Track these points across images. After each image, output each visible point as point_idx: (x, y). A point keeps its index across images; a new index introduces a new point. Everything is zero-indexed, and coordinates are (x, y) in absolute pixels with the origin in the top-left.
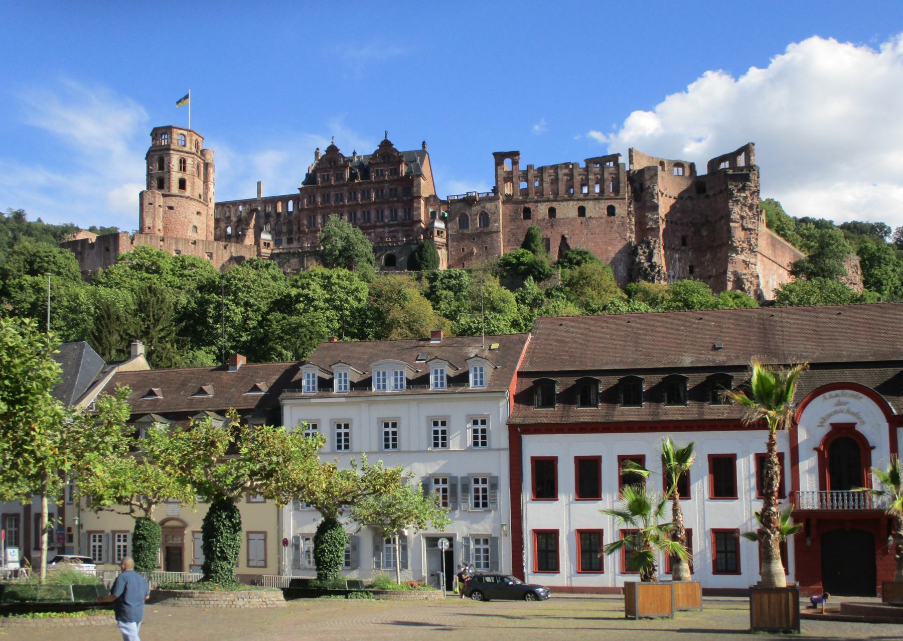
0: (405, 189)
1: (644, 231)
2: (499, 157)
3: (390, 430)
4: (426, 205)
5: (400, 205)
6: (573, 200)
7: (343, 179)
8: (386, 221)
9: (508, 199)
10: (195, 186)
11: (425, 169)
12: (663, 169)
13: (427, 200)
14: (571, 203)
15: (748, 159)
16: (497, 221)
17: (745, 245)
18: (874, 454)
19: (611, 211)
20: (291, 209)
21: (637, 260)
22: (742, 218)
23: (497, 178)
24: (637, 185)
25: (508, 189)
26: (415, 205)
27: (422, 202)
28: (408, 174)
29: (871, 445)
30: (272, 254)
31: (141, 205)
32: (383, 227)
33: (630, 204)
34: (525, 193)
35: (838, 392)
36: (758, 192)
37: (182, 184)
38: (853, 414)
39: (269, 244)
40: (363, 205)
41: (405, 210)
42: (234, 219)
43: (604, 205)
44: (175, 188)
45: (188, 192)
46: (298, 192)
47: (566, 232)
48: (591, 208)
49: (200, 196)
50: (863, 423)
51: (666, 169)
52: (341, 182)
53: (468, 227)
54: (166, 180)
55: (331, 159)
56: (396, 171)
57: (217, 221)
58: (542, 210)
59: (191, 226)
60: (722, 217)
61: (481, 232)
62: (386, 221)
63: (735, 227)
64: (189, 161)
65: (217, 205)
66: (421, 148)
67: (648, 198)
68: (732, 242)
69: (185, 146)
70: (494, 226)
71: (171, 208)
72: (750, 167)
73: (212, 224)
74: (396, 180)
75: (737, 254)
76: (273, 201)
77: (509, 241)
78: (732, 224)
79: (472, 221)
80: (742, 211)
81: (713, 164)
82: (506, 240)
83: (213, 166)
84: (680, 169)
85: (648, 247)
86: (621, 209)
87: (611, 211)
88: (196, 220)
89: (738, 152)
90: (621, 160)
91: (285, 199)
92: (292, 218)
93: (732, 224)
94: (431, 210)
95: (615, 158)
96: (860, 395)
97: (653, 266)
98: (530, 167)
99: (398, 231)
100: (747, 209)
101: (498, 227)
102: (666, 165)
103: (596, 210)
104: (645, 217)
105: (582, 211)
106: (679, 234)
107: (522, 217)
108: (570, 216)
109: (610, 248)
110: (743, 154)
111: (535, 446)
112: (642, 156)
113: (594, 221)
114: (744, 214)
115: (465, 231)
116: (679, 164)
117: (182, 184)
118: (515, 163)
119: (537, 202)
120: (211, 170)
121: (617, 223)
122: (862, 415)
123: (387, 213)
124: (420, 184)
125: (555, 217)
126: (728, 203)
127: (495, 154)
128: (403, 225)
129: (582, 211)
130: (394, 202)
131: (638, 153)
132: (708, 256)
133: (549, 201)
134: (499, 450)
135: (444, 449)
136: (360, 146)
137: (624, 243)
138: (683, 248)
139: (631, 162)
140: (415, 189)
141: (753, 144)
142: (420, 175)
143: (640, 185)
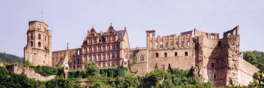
0: (117, 46)
1: (198, 61)
11: (125, 38)
13: (124, 50)
19: (186, 54)
22: (233, 56)
24: (196, 44)
28: (118, 40)
36: (239, 45)
37: (39, 44)
41: (117, 54)
43: (184, 52)
44: (37, 46)
48: (181, 53)
54: (33, 43)
60: (226, 56)
61: (141, 63)
63: (230, 60)
64: (42, 35)
66: (124, 29)
68: (229, 65)
79: (138, 58)
81: (225, 34)
82: (150, 66)
84: (214, 36)
85: (198, 68)
86: (190, 54)
87: (186, 54)
89: (234, 30)
93: (229, 58)
95: (190, 32)
97: (199, 76)
99: (114, 62)
100: (235, 53)
103: (181, 53)
105: (176, 54)
110: (235, 30)
113: (180, 58)
114: (233, 54)
116: (213, 34)
117: (39, 44)
125: (166, 56)
126: (228, 50)
128: (116, 60)
129: (176, 54)
130: (113, 51)
136: (102, 29)
140: (120, 46)
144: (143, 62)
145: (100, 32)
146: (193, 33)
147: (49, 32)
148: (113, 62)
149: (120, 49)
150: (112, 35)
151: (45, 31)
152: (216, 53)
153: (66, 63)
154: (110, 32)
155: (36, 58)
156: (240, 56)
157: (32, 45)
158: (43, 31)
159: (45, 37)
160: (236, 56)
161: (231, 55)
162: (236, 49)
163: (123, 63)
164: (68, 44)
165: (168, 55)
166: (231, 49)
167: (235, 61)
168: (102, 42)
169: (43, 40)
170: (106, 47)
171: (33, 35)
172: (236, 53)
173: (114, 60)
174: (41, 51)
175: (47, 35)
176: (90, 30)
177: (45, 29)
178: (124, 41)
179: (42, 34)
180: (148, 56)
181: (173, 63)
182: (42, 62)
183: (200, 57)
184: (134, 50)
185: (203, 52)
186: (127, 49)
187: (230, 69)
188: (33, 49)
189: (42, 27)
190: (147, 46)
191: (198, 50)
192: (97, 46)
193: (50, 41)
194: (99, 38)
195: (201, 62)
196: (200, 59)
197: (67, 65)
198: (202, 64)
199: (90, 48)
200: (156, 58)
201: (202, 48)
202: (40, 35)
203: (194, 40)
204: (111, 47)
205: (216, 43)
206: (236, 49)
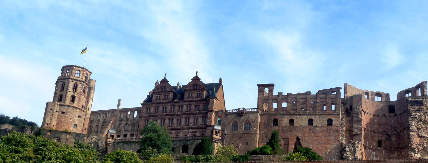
1: (352, 135)
2: (261, 87)
4: (216, 115)
5: (201, 115)
6: (306, 115)
10: (81, 101)
11: (218, 95)
12: (368, 98)
13: (216, 113)
14: (304, 116)
16: (256, 126)
17: (420, 147)
19: (330, 122)
20: (135, 116)
21: (345, 154)
22: (418, 129)
25: (265, 108)
26: (209, 115)
28: (206, 97)
31: (46, 110)
32: (188, 129)
33: (342, 118)
37: (73, 98)
39: (113, 136)
40: (177, 115)
41: (203, 118)
42: (101, 121)
43: (325, 118)
44: (68, 102)
45: (75, 104)
46: (141, 106)
47: (300, 135)
48: (319, 121)
49: (83, 107)
51: (370, 97)
53: (237, 130)
54: (64, 97)
56: (200, 95)
57: (91, 122)
58: (285, 121)
59: (73, 124)
60: (405, 129)
62: (191, 125)
63: (413, 135)
66: (218, 82)
69: (79, 77)
73: (87, 123)
74: (199, 101)
75: (415, 153)
76: (125, 111)
77: (263, 139)
78: (411, 133)
79: (240, 126)
80: (418, 125)
81: (402, 95)
82: (261, 139)
83: (94, 90)
84: (380, 98)
87: (330, 122)
88: (77, 121)
89: (418, 87)
91: (133, 110)
93: (411, 133)
94: (219, 119)
95: (337, 90)
98: (280, 94)
99: (196, 132)
101: (256, 131)
102: (370, 94)
104: (352, 127)
105: (311, 122)
106: (376, 139)
107: (272, 124)
108: (303, 125)
109: (328, 146)
113: (319, 129)
115: (235, 132)
116: (378, 94)
117: (73, 98)
118: (271, 91)
119: (282, 115)
120: (92, 91)
123: (192, 120)
124: (213, 103)
125: (293, 125)
127: (259, 85)
128: (200, 128)
129: (311, 122)
130: (196, 114)
131: (350, 86)
132: (396, 154)
133: (290, 114)
136: (180, 78)
137: (337, 143)
138: (379, 148)
139: (345, 92)
140: (210, 106)
141: (426, 82)
142: (214, 97)
143: (350, 107)
144: (248, 132)
145: (176, 85)
146: (342, 91)
148: (194, 130)
149: (209, 111)
150: (195, 90)
152: (386, 124)
154: (194, 84)
159: (85, 89)
160: (424, 130)
162: (423, 118)
163: (212, 132)
165: (296, 124)
168: (178, 100)
170: (185, 108)
173: (197, 128)
175: (88, 86)
176: (160, 80)
177: (86, 78)
180: (259, 124)
181: (305, 137)
182: (73, 125)
183: (357, 128)
185: (361, 120)
186: (222, 111)
187: (413, 150)
188: (60, 105)
189: (81, 74)
191: (353, 117)
192: (169, 104)
195: (357, 137)
196: (356, 131)
199: (157, 109)
200: (273, 127)
201: (360, 114)
202: (75, 86)
203: (345, 101)
204: (193, 107)
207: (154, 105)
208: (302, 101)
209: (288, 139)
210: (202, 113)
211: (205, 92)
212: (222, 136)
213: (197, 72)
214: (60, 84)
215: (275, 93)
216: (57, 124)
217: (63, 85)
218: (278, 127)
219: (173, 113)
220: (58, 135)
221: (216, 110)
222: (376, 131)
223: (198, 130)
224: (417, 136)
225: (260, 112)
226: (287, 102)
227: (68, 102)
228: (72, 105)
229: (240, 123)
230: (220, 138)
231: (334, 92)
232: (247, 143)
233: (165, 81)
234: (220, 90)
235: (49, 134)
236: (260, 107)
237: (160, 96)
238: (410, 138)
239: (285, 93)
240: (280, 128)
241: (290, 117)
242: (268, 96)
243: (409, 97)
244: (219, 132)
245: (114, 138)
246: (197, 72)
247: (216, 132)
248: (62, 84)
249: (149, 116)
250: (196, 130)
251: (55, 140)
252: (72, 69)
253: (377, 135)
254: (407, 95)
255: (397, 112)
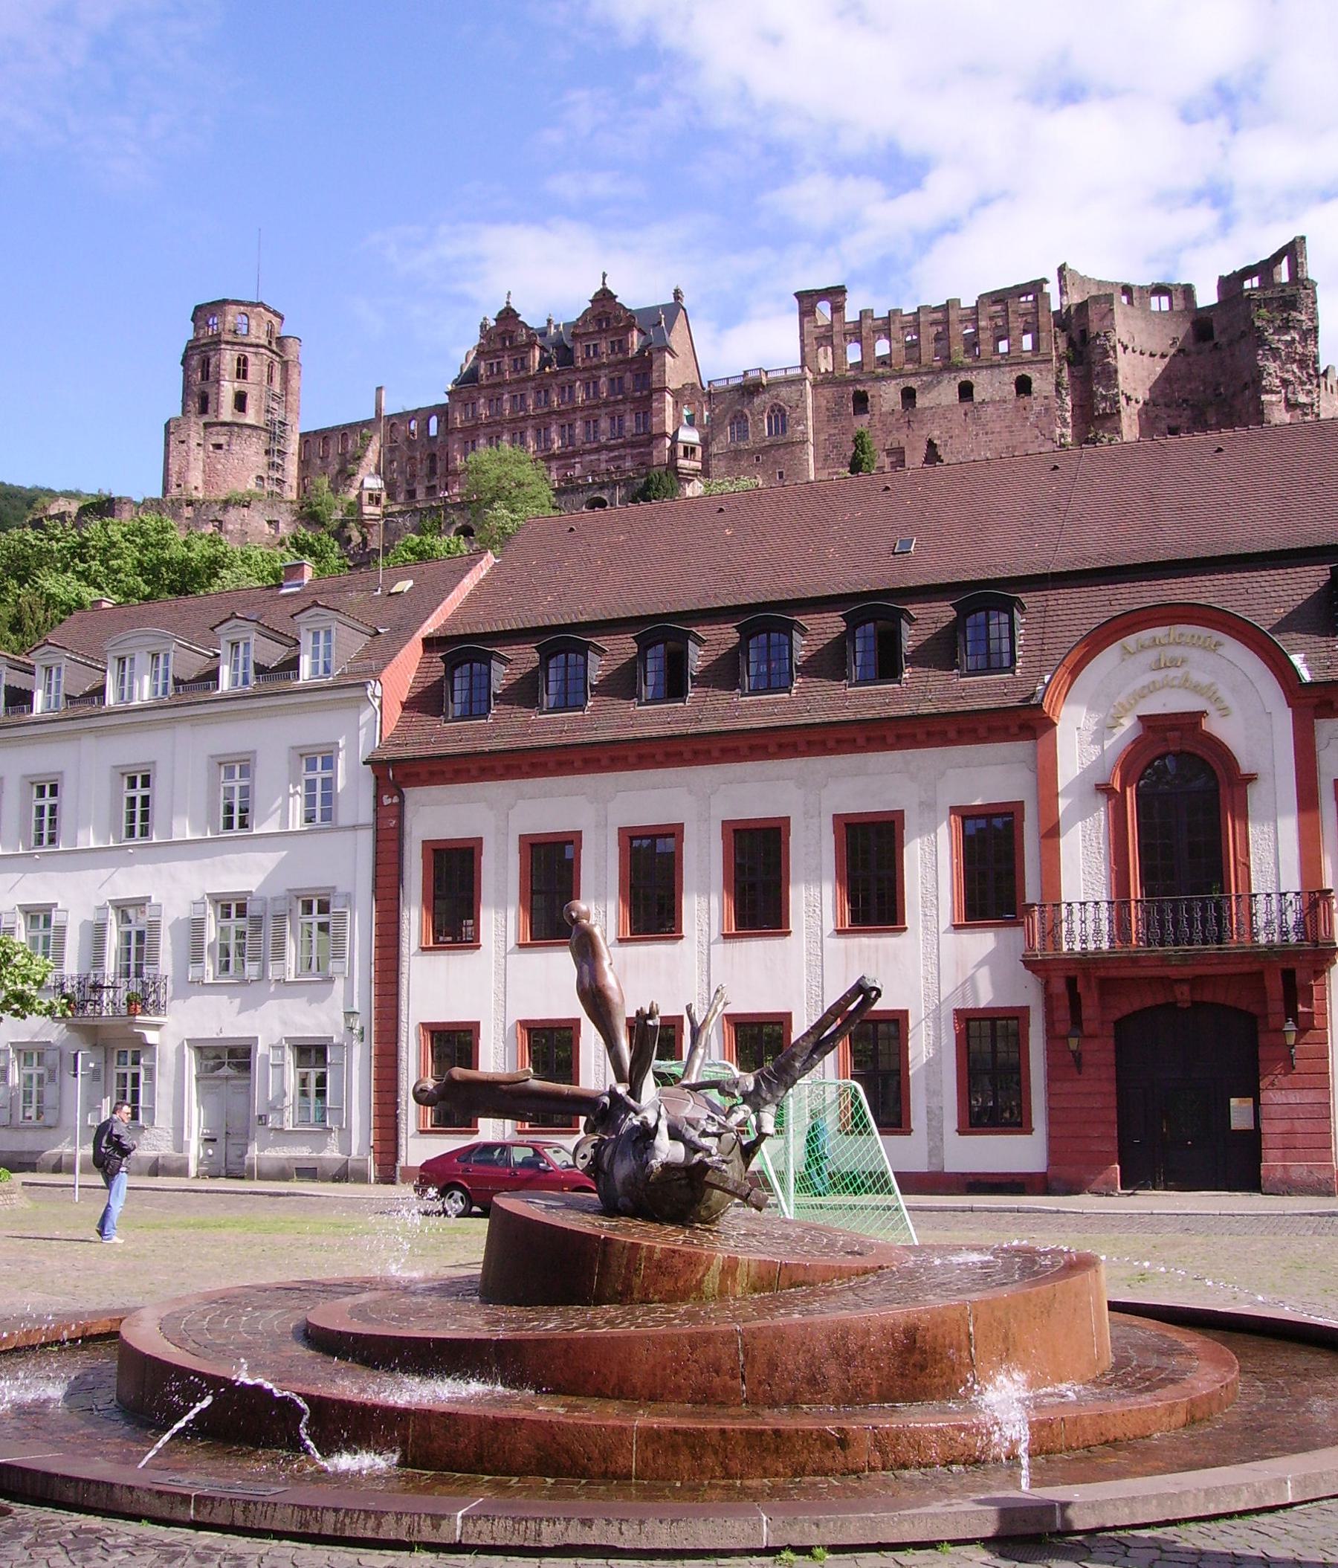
0: (640, 381)
2: (807, 301)
3: (139, 793)
5: (629, 406)
7: (525, 368)
8: (603, 439)
9: (825, 381)
11: (676, 339)
12: (1130, 302)
13: (675, 393)
15: (1294, 268)
18: (1256, 796)
19: (1023, 386)
22: (1285, 383)
23: (802, 341)
24: (1076, 336)
25: (825, 364)
26: (655, 405)
27: (669, 398)
28: (641, 351)
29: (1245, 767)
30: (385, 515)
32: (597, 450)
34: (858, 366)
35: (1159, 632)
36: (1316, 329)
37: (240, 401)
38: (1197, 689)
40: (561, 414)
43: (1010, 376)
44: (227, 413)
45: (250, 417)
46: (445, 400)
47: (937, 433)
50: (1225, 712)
52: (522, 374)
55: (505, 333)
56: (622, 346)
58: (887, 395)
60: (1246, 386)
63: (1272, 403)
65: (302, 435)
66: (672, 301)
67: (1096, 357)
70: (795, 432)
71: (219, 447)
72: (1297, 279)
74: (621, 362)
78: (1264, 397)
79: (755, 424)
81: (1230, 285)
84: (1165, 300)
86: (1042, 384)
87: (1023, 386)
89: (1276, 258)
90: (1047, 288)
91: (423, 415)
92: (435, 449)
93: (1264, 397)
94: (686, 413)
95: (1036, 287)
96: (1218, 636)
98: (865, 314)
99: (622, 458)
100: (1295, 366)
104: (1092, 395)
105: (966, 391)
107: (851, 410)
110: (1285, 260)
111: (435, 815)
112: (1084, 280)
113: (990, 409)
114: (1286, 376)
116: (1160, 290)
117: (240, 401)
118: (837, 309)
120: (293, 372)
121: (1036, 408)
122: (1224, 693)
123: (604, 424)
124: (664, 365)
127: (798, 295)
128: (632, 445)
129: (966, 391)
130: (617, 402)
134: (354, 827)
135: (243, 833)
140: (655, 375)
141: (1303, 238)
143: (1080, 336)
146: (1052, 288)
147: (292, 346)
148: (616, 453)
150: (604, 331)
151: (270, 343)
153: (370, 475)
155: (219, 467)
156: (1323, 385)
157: (204, 410)
158: (257, 341)
159: (271, 366)
160: (1302, 383)
161: (1277, 382)
163: (673, 451)
164: (379, 389)
165: (921, 402)
166: (1271, 349)
167: (1299, 412)
169: (259, 384)
171: (213, 361)
172: (1301, 368)
173: (623, 446)
174: (248, 432)
177: (270, 333)
178: (673, 354)
179: (256, 353)
180: (810, 413)
183: (1104, 398)
184: (732, 382)
185: (1116, 371)
188: (207, 425)
189: (253, 323)
190: (803, 359)
191: (1090, 364)
193: (294, 383)
194: (542, 348)
197: (374, 483)
198: (1119, 432)
199: (494, 401)
200: (854, 419)
202: (242, 362)
203: (1062, 320)
205: (1181, 330)
206: (1300, 350)
207: (484, 392)
208: (933, 331)
209: (901, 451)
210: (634, 400)
211: (635, 333)
212: (705, 461)
213: (604, 276)
214: (195, 361)
215: (851, 315)
216: (205, 483)
217: (205, 363)
218: (868, 416)
219: (546, 410)
220: (216, 511)
221: (672, 385)
222: (1161, 401)
223: (628, 451)
224: (1283, 404)
225: (810, 375)
226: (889, 337)
227: (227, 413)
228: (240, 421)
229: (752, 414)
230: (699, 465)
231: (1027, 294)
232: (781, 474)
233: (508, 316)
234: (679, 324)
235: (188, 512)
236: (808, 360)
237: (498, 363)
238: (1262, 413)
239: (881, 312)
240: (876, 417)
241: (903, 383)
242: (831, 326)
243: (1252, 289)
244: (693, 450)
245: (384, 500)
246: (604, 276)
247: (686, 448)
248: (199, 362)
249: (476, 427)
250: (622, 451)
251: (210, 529)
252: (224, 314)
253: (1163, 412)
254: (1247, 284)
255: (1220, 339)
